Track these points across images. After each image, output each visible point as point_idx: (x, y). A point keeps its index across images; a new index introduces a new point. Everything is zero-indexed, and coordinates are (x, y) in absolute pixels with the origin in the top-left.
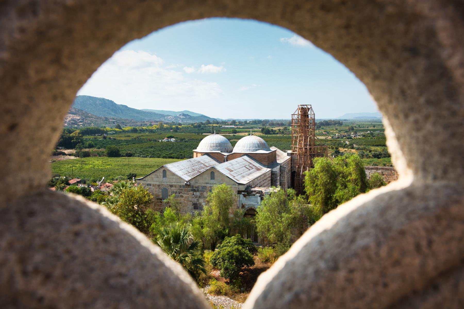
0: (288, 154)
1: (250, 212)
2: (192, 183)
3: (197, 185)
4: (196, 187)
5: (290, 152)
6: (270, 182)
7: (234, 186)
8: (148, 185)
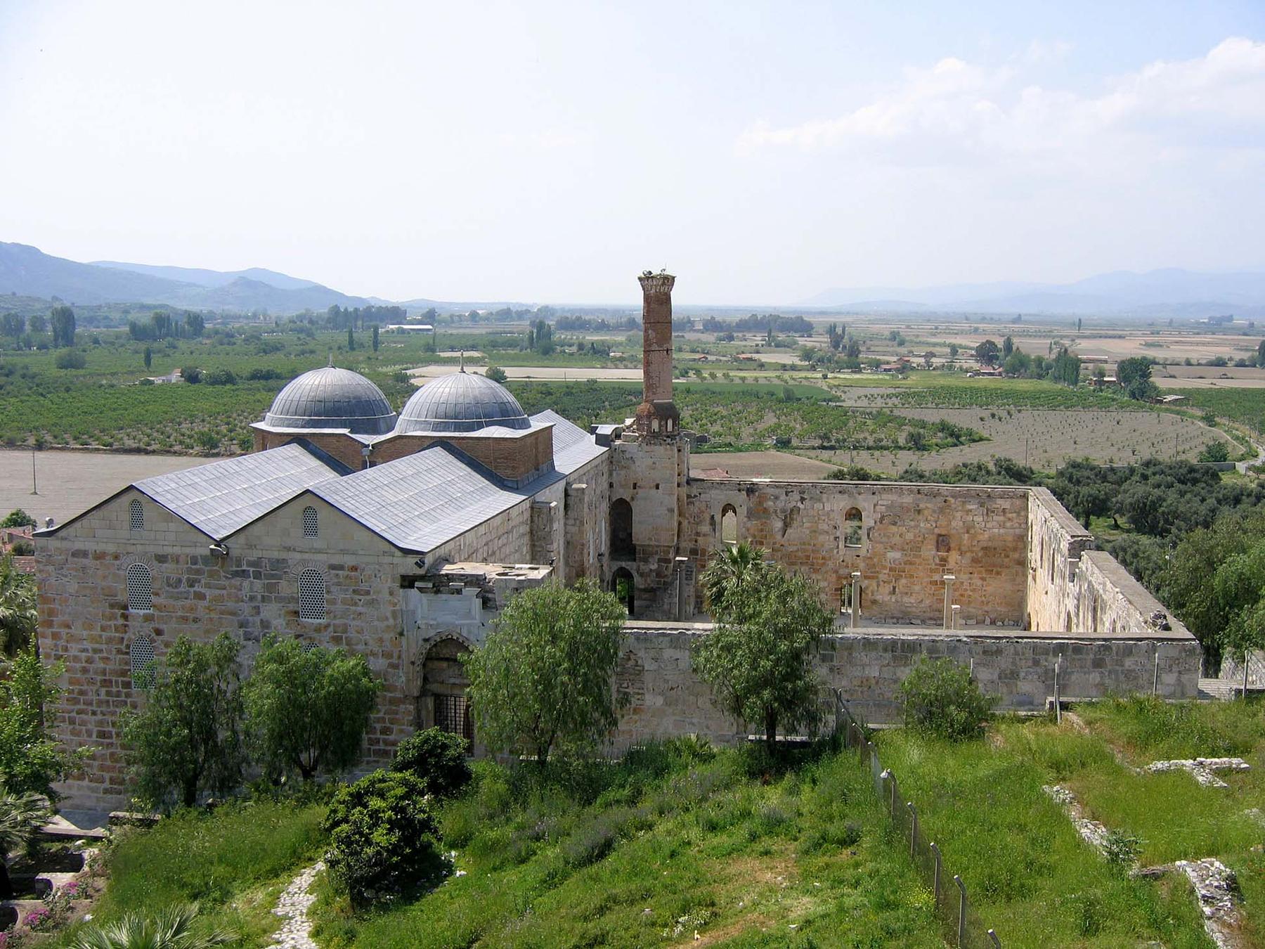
0: (601, 440)
1: (445, 652)
2: (236, 548)
3: (254, 555)
4: (250, 564)
5: (606, 429)
6: (526, 539)
7: (387, 559)
8: (75, 554)
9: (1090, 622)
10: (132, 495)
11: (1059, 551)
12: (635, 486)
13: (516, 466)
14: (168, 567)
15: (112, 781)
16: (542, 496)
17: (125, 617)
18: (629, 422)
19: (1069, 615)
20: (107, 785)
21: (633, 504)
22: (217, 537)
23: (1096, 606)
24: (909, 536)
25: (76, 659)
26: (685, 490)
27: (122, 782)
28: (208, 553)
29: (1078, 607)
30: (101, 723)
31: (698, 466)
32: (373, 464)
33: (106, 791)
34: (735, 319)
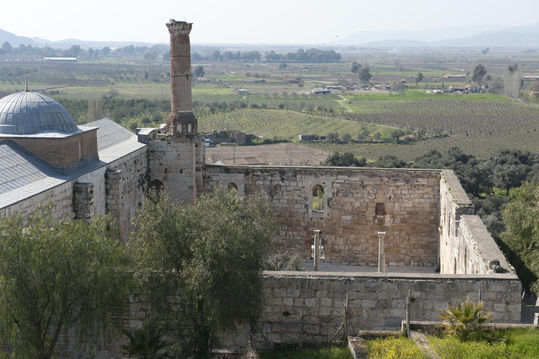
0: (142, 139)
5: (146, 131)
12: (166, 171)
16: (83, 179)
26: (201, 174)
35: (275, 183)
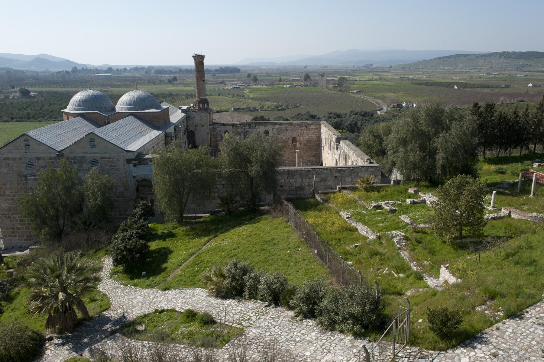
0: (183, 111)
2: (66, 154)
3: (73, 155)
4: (72, 159)
5: (185, 108)
7: (122, 154)
8: (4, 159)
9: (344, 162)
10: (25, 137)
11: (332, 141)
12: (195, 126)
13: (158, 121)
14: (41, 162)
15: (27, 236)
17: (26, 180)
18: (192, 105)
19: (336, 160)
20: (25, 238)
21: (195, 132)
22: (59, 150)
23: (346, 157)
24: (284, 138)
25: (9, 196)
26: (211, 127)
27: (31, 236)
28: (56, 156)
29: (340, 158)
30: (21, 217)
31: (217, 118)
32: (109, 123)
33: (25, 240)
34: (214, 69)
35: (246, 130)
